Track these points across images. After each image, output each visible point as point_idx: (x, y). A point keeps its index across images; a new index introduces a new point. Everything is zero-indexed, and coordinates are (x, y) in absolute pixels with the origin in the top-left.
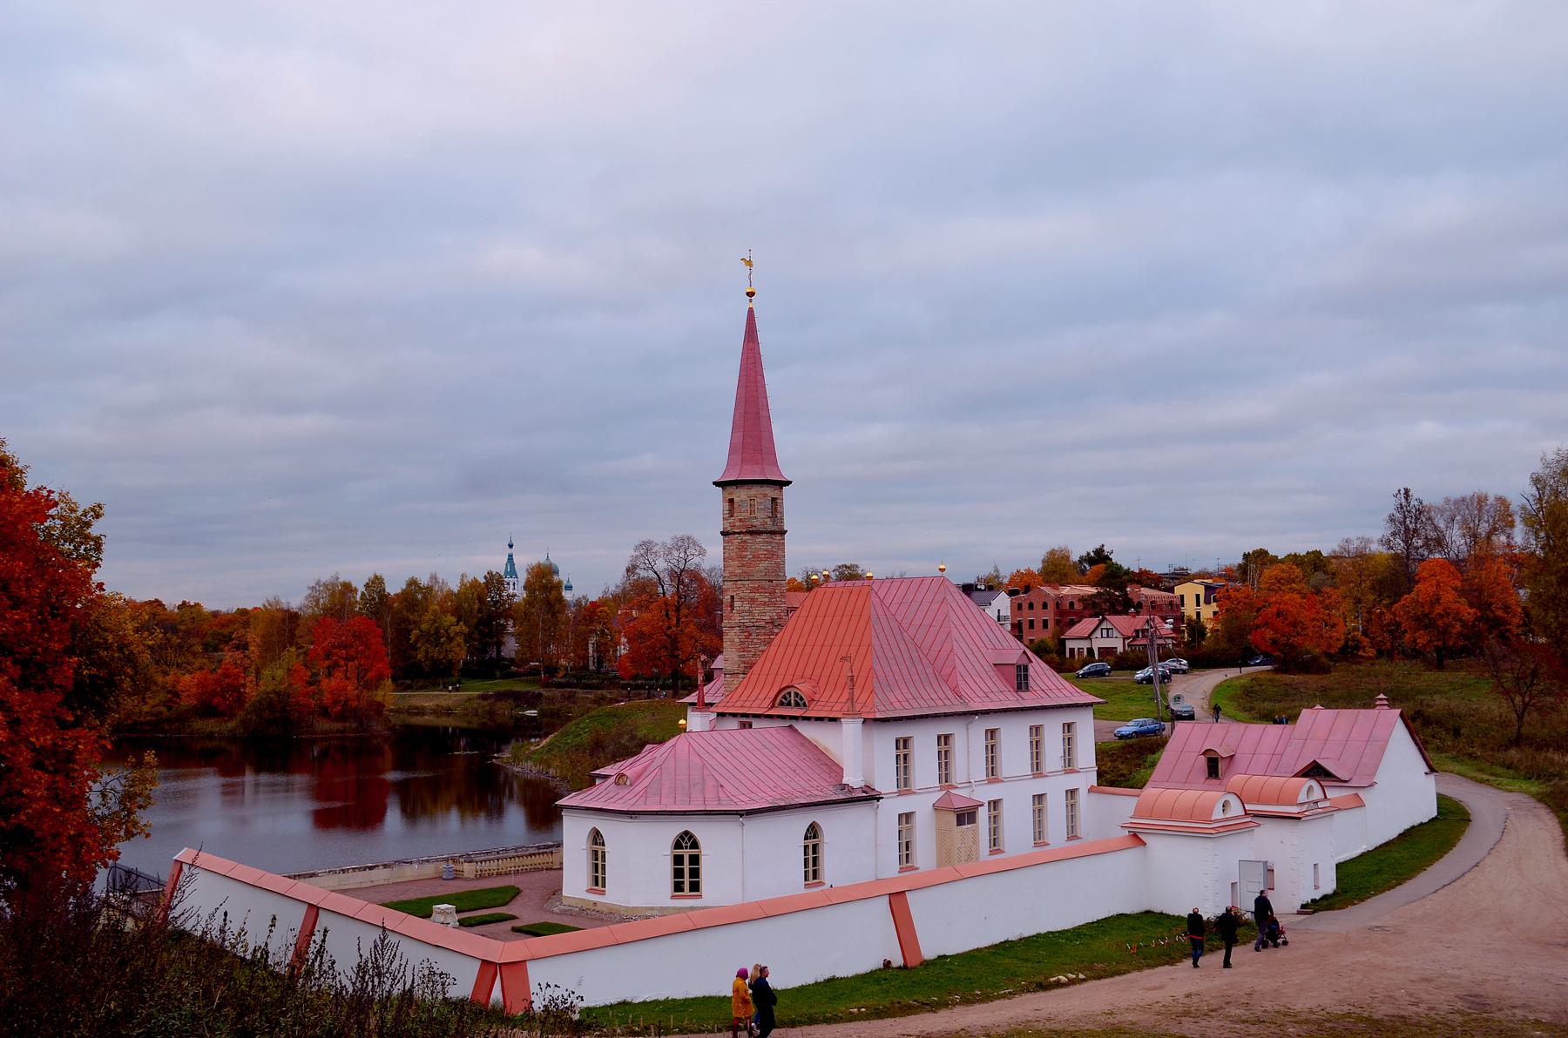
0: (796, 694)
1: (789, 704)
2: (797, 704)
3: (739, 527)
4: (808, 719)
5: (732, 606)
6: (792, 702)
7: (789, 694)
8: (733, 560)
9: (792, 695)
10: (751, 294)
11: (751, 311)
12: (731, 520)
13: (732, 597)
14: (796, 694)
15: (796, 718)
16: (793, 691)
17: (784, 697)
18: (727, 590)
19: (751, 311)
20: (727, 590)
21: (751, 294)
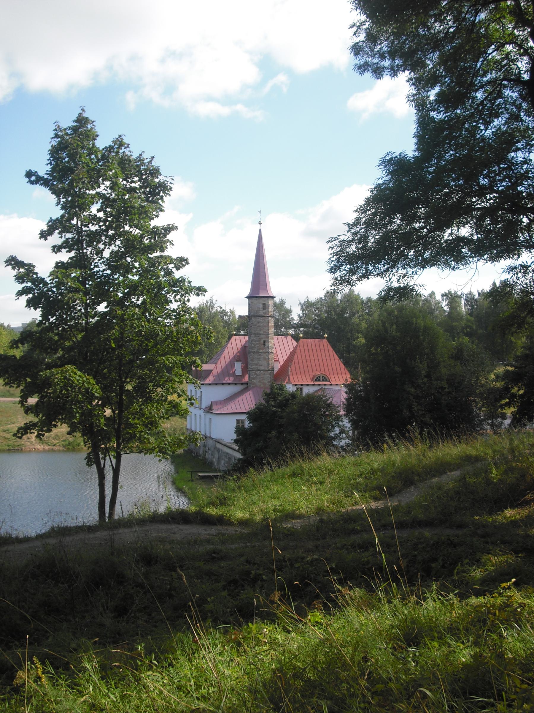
0: (323, 377)
1: (319, 380)
2: (323, 380)
4: (331, 385)
5: (264, 345)
7: (320, 377)
10: (260, 223)
11: (260, 230)
12: (264, 311)
13: (264, 342)
14: (323, 377)
15: (325, 385)
17: (317, 378)
18: (262, 338)
19: (260, 230)
20: (262, 338)
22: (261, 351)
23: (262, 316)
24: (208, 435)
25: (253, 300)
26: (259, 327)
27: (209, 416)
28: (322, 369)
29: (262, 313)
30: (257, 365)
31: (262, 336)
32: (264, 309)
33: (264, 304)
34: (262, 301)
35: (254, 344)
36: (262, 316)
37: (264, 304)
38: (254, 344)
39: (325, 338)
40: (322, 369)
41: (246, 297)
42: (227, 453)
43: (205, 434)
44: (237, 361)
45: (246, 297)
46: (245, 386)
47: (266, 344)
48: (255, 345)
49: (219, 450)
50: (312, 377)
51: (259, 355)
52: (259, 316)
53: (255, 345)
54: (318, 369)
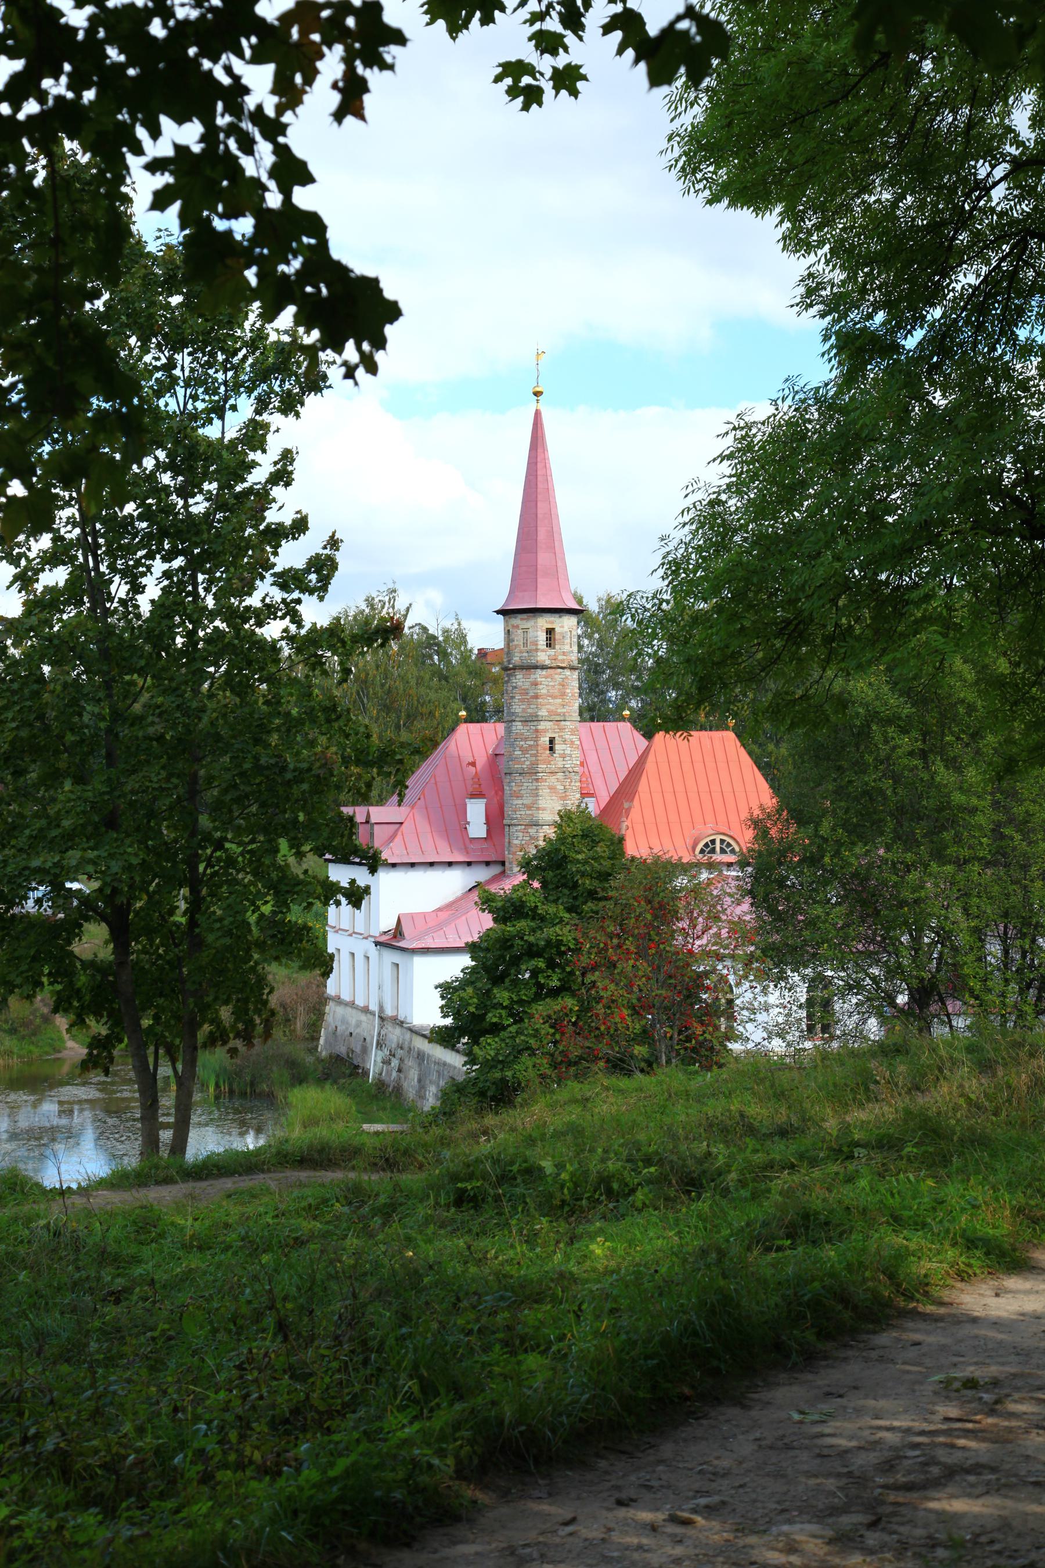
0: (722, 841)
2: (723, 851)
3: (563, 661)
5: (551, 749)
6: (718, 849)
7: (713, 842)
8: (554, 697)
9: (718, 842)
10: (537, 394)
11: (538, 414)
12: (551, 652)
13: (552, 741)
16: (718, 838)
17: (706, 845)
18: (545, 731)
19: (538, 414)
20: (545, 731)
21: (537, 394)
22: (542, 767)
23: (544, 667)
24: (389, 1012)
25: (517, 621)
26: (536, 697)
27: (390, 957)
28: (722, 818)
29: (543, 657)
30: (529, 808)
31: (542, 726)
32: (549, 645)
33: (550, 632)
34: (544, 622)
35: (521, 748)
36: (544, 667)
37: (550, 632)
38: (521, 748)
39: (727, 729)
40: (722, 818)
41: (498, 612)
42: (445, 1064)
43: (381, 1008)
44: (473, 796)
45: (498, 612)
46: (495, 870)
47: (557, 747)
48: (525, 751)
49: (421, 1056)
50: (689, 842)
51: (537, 780)
52: (536, 667)
53: (525, 751)
54: (709, 817)
